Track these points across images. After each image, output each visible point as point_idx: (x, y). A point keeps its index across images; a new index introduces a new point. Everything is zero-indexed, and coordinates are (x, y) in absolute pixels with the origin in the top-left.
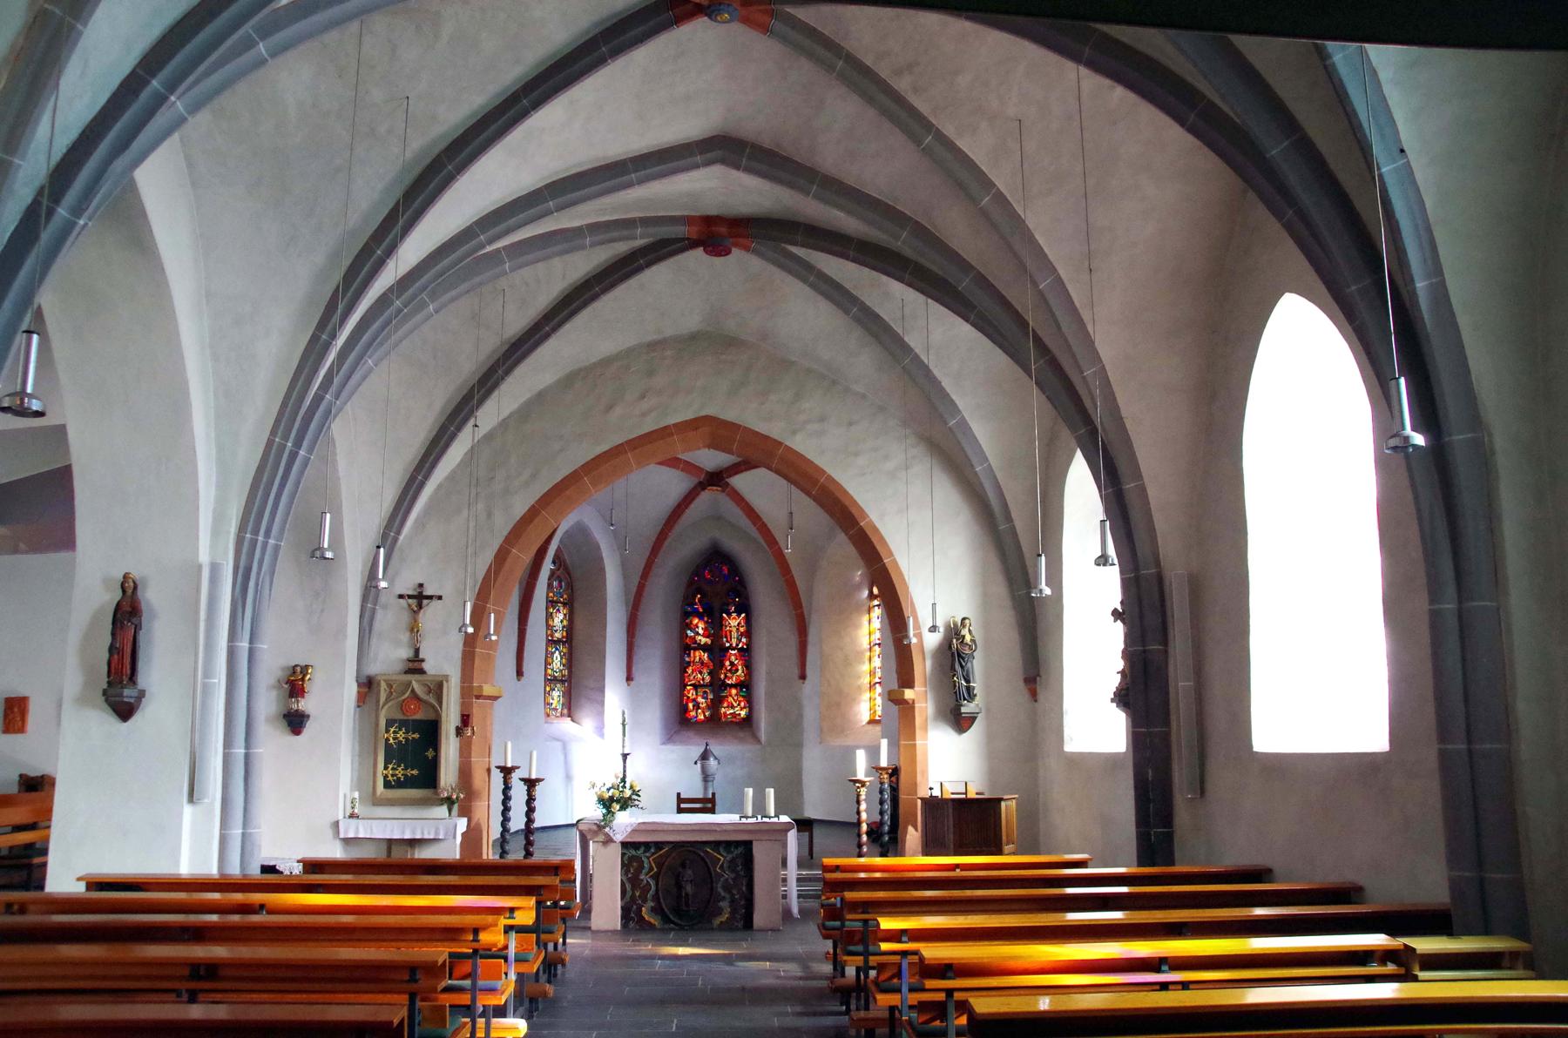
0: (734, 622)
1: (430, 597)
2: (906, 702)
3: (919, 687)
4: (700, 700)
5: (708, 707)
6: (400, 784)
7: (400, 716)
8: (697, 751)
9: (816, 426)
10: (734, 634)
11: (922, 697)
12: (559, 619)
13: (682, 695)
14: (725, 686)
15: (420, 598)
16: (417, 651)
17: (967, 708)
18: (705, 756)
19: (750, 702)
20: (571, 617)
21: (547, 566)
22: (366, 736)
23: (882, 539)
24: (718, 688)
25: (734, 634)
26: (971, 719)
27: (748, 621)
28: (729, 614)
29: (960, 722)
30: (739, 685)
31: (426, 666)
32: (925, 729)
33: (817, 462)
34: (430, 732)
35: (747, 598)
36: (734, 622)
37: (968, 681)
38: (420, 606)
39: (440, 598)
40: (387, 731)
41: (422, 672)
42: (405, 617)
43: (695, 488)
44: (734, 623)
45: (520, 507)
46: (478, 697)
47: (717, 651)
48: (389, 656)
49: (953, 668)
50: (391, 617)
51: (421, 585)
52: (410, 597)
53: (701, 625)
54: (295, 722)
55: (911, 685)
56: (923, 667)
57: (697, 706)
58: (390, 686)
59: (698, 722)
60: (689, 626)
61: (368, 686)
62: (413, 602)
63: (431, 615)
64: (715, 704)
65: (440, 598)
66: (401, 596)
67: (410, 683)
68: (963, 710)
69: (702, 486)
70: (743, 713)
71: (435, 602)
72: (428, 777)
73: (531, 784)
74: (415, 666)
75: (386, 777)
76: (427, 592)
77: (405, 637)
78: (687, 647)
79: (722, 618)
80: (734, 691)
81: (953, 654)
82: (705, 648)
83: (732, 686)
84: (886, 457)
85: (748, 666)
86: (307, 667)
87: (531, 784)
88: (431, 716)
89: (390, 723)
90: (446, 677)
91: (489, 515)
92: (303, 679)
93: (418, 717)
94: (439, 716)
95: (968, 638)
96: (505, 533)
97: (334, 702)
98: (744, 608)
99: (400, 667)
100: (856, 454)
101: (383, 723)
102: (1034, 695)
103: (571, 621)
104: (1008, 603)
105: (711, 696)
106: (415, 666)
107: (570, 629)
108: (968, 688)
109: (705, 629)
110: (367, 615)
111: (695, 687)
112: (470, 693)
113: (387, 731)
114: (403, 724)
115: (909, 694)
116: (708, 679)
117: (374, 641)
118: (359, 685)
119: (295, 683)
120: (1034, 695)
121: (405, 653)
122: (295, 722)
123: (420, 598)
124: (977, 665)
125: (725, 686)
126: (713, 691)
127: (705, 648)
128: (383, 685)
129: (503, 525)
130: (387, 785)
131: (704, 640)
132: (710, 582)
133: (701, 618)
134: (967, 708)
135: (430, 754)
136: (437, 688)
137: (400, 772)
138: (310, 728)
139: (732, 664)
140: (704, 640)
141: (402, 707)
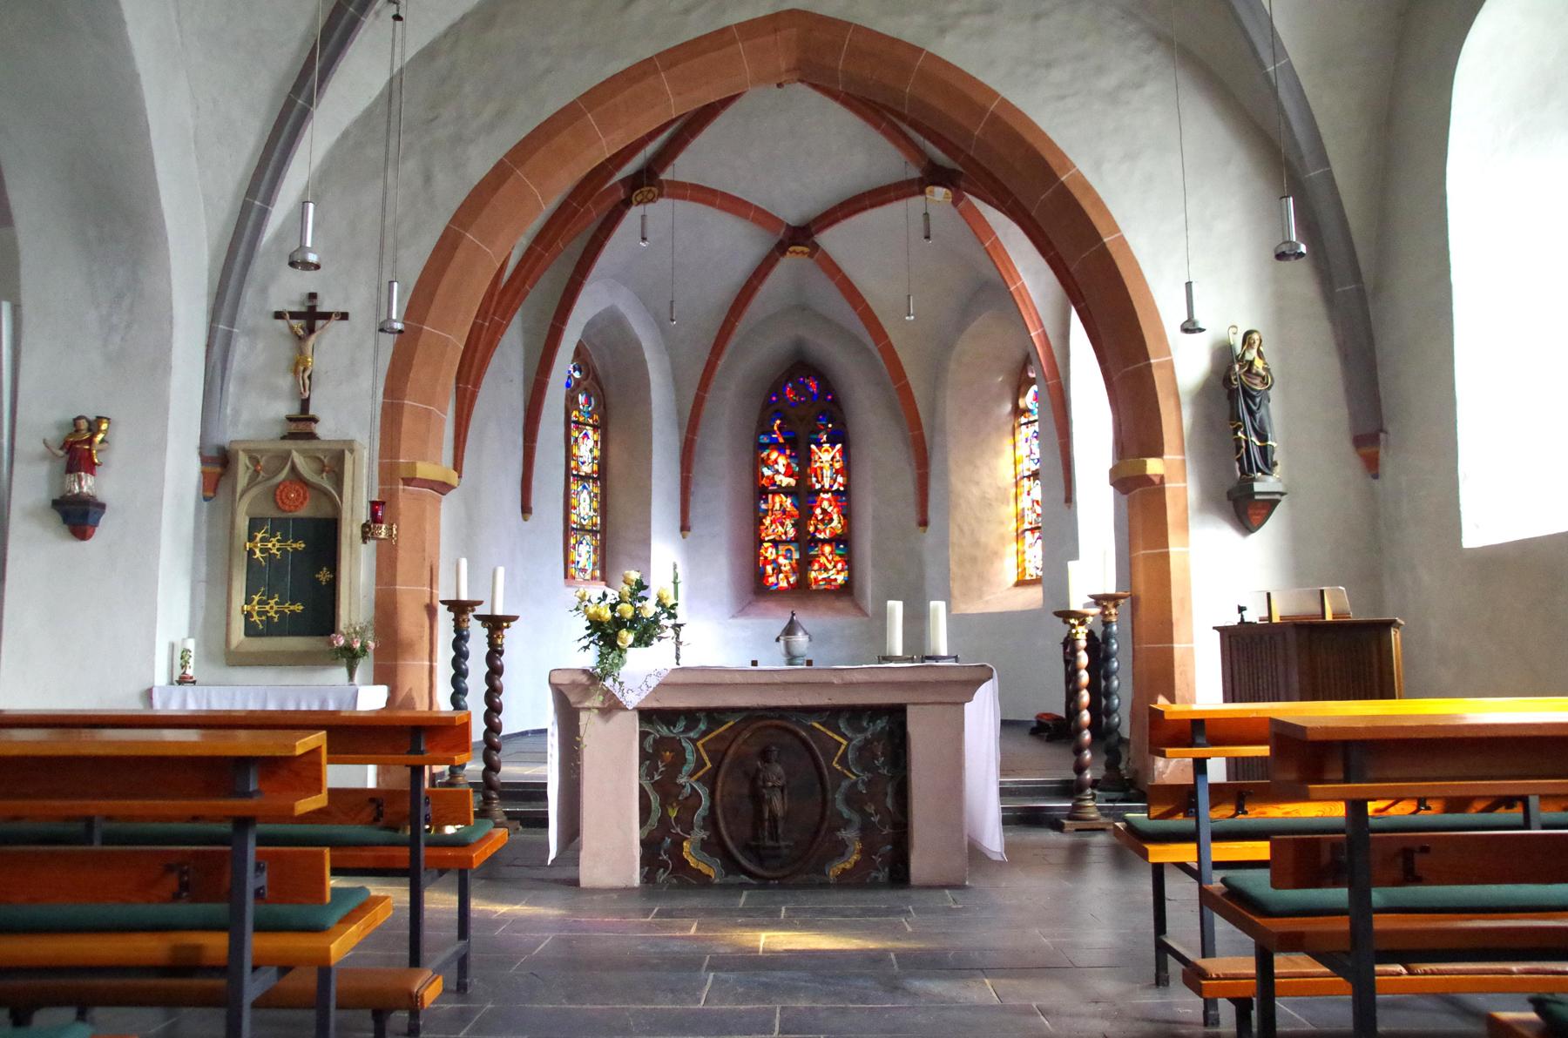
1: (327, 316)
2: (1146, 480)
3: (1171, 455)
4: (781, 560)
5: (794, 570)
6: (271, 629)
7: (271, 512)
8: (778, 624)
9: (979, 21)
10: (827, 473)
11: (1177, 470)
12: (587, 449)
13: (757, 555)
14: (818, 542)
15: (311, 317)
16: (305, 404)
17: (1264, 485)
18: (790, 630)
19: (849, 561)
21: (564, 366)
22: (215, 550)
23: (1098, 203)
24: (806, 543)
25: (827, 473)
26: (1270, 505)
27: (845, 453)
28: (819, 445)
29: (1244, 509)
30: (835, 540)
31: (320, 430)
32: (1185, 527)
33: (980, 78)
34: (322, 541)
35: (844, 424)
36: (826, 457)
37: (1263, 437)
38: (311, 330)
39: (344, 316)
40: (251, 538)
41: (312, 436)
42: (286, 349)
44: (826, 457)
45: (479, 165)
46: (408, 481)
47: (804, 495)
48: (256, 414)
49: (1235, 417)
50: (257, 350)
51: (313, 296)
52: (294, 315)
53: (782, 461)
54: (78, 516)
55: (1158, 453)
56: (1179, 420)
57: (778, 570)
58: (255, 461)
59: (782, 590)
60: (765, 462)
61: (219, 465)
62: (297, 324)
63: (329, 343)
65: (344, 316)
66: (279, 315)
67: (289, 453)
68: (1257, 487)
70: (841, 578)
71: (334, 325)
72: (319, 614)
73: (495, 624)
74: (301, 425)
75: (248, 616)
76: (324, 306)
77: (285, 382)
78: (762, 491)
79: (810, 452)
80: (827, 549)
81: (1233, 389)
82: (787, 491)
83: (824, 542)
84: (1100, 70)
85: (847, 515)
86: (99, 419)
87: (495, 624)
88: (325, 511)
89: (255, 524)
90: (350, 445)
91: (428, 179)
92: (90, 441)
93: (304, 512)
94: (337, 509)
95: (1259, 364)
96: (454, 206)
97: (159, 487)
98: (839, 436)
99: (278, 430)
100: (1048, 65)
101: (243, 524)
102: (1372, 465)
103: (604, 450)
104: (1319, 308)
105: (796, 556)
106: (301, 425)
108: (1264, 451)
109: (788, 466)
110: (217, 349)
111: (776, 543)
112: (392, 473)
113: (251, 538)
114: (278, 526)
115: (1154, 466)
116: (791, 533)
117: (232, 388)
118: (205, 460)
119: (77, 450)
120: (1372, 465)
121: (286, 407)
122: (78, 516)
123: (311, 317)
124: (1275, 411)
125: (818, 542)
126: (800, 550)
127: (787, 491)
128: (243, 460)
129: (451, 192)
130: (251, 630)
132: (794, 404)
133: (782, 451)
134: (1264, 485)
135: (324, 576)
136: (335, 463)
137: (272, 608)
138: (106, 528)
139: (824, 511)
141: (276, 495)
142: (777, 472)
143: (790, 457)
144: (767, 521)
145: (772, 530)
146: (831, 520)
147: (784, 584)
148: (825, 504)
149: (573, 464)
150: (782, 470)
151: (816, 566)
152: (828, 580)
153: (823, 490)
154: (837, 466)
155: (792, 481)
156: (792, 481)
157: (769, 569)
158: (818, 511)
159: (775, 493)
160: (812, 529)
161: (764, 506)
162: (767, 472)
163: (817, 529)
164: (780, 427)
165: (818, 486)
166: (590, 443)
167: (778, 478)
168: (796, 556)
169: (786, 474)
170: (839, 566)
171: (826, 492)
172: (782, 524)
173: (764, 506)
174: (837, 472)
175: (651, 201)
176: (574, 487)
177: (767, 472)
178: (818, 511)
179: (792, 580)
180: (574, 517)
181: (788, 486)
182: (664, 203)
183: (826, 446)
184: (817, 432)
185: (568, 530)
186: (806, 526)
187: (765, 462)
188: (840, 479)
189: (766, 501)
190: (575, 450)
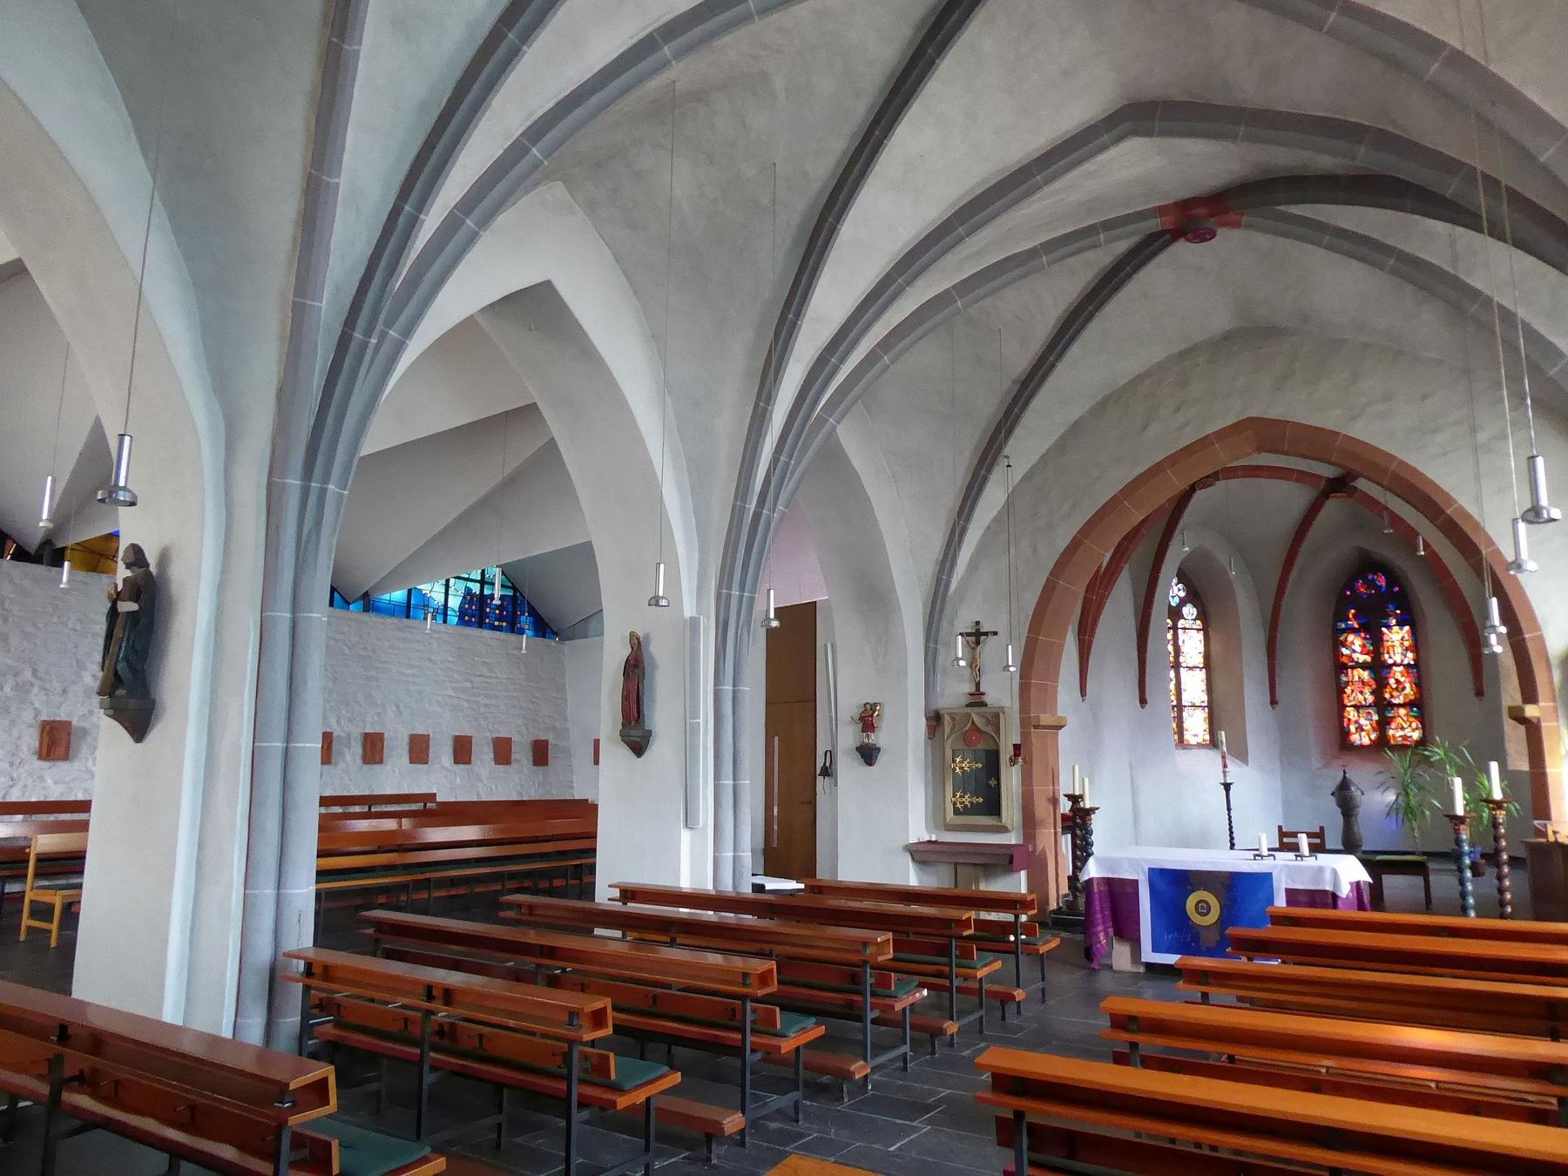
4: (1362, 721)
10: (1399, 650)
13: (1341, 717)
19: (1423, 719)
24: (1383, 706)
27: (1413, 633)
28: (1389, 627)
30: (1408, 705)
36: (1397, 637)
47: (1379, 669)
57: (1360, 729)
59: (1362, 746)
60: (1344, 644)
64: (1383, 725)
69: (1324, 496)
70: (1416, 735)
79: (1382, 634)
80: (1402, 711)
82: (1364, 666)
83: (1400, 705)
105: (1376, 717)
109: (1363, 646)
111: (1357, 707)
116: (1370, 699)
126: (1378, 713)
127: (1364, 666)
131: (1362, 658)
139: (1398, 681)
144: (1348, 690)
145: (1353, 696)
147: (1366, 741)
148: (1398, 676)
150: (1358, 649)
151: (1393, 725)
152: (1405, 737)
153: (1395, 664)
154: (1407, 644)
155: (1368, 658)
156: (1368, 658)
157: (1353, 728)
158: (1392, 681)
159: (1353, 668)
160: (1387, 696)
162: (1345, 651)
167: (1355, 656)
168: (1376, 717)
174: (1407, 649)
179: (1373, 736)
181: (1365, 662)
183: (1396, 628)
186: (1382, 694)
187: (1344, 644)
188: (1410, 655)
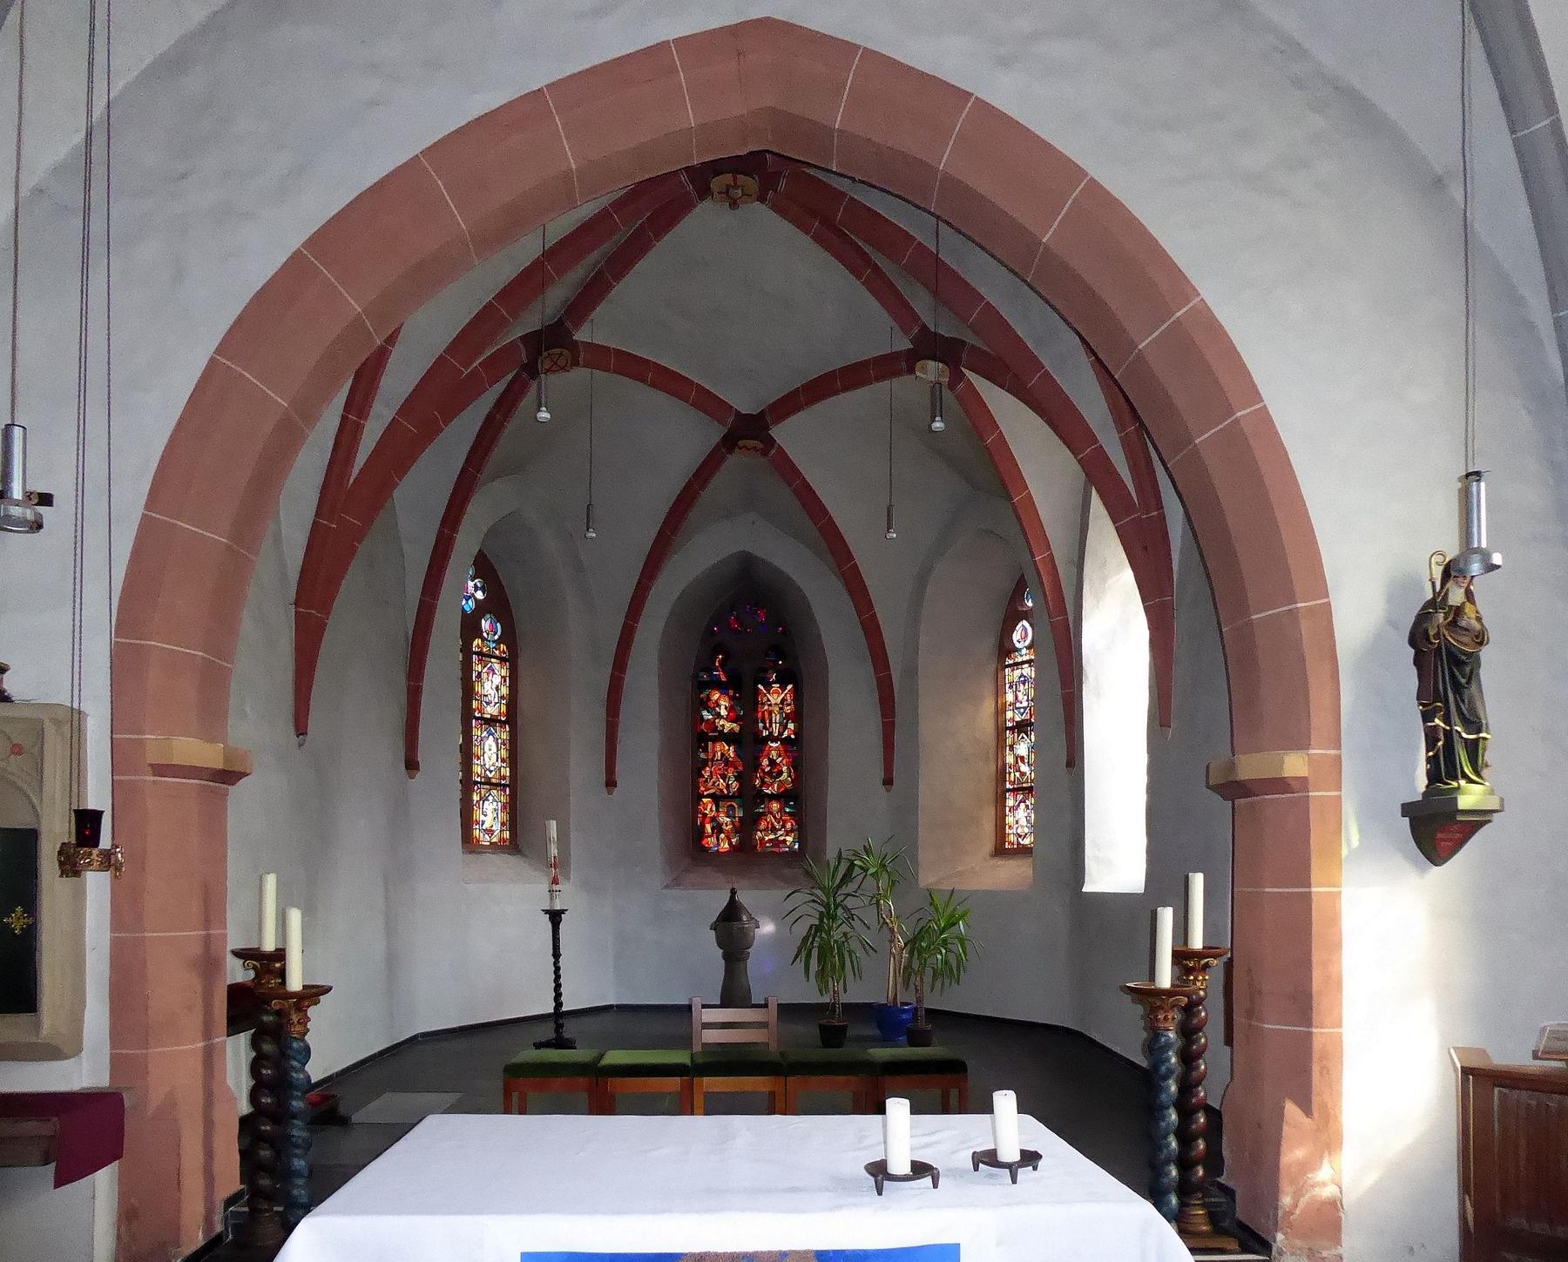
0: (776, 698)
4: (724, 819)
5: (736, 830)
10: (776, 718)
12: (492, 686)
13: (696, 811)
20: (513, 679)
24: (750, 799)
25: (776, 718)
27: (797, 693)
28: (768, 686)
36: (776, 698)
43: (716, 449)
44: (775, 699)
47: (749, 742)
53: (724, 703)
57: (718, 829)
60: (705, 704)
64: (747, 826)
78: (703, 737)
80: (775, 806)
82: (730, 738)
83: (772, 797)
85: (796, 765)
103: (513, 688)
107: (512, 702)
109: (730, 709)
111: (717, 798)
116: (735, 785)
127: (730, 738)
131: (728, 726)
139: (772, 763)
140: (728, 726)
142: (719, 716)
143: (732, 699)
146: (781, 773)
149: (475, 704)
150: (724, 712)
151: (763, 825)
152: (776, 843)
153: (771, 738)
154: (788, 709)
157: (708, 828)
158: (765, 762)
159: (715, 740)
161: (703, 756)
162: (707, 715)
163: (763, 783)
164: (722, 663)
165: (765, 733)
166: (497, 680)
169: (728, 719)
170: (789, 825)
171: (775, 740)
172: (724, 777)
173: (703, 756)
174: (788, 717)
175: (563, 369)
176: (476, 732)
177: (707, 715)
178: (765, 762)
179: (734, 841)
180: (477, 769)
181: (732, 732)
182: (579, 374)
184: (765, 671)
185: (468, 784)
188: (791, 726)
189: (705, 750)
190: (478, 688)
